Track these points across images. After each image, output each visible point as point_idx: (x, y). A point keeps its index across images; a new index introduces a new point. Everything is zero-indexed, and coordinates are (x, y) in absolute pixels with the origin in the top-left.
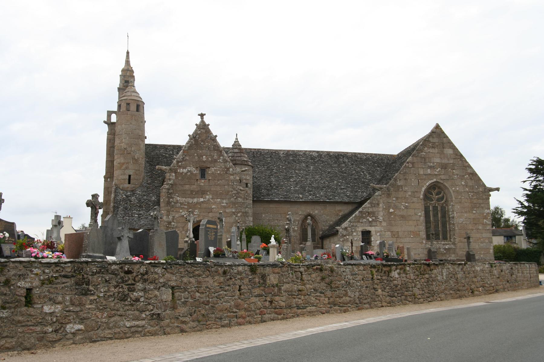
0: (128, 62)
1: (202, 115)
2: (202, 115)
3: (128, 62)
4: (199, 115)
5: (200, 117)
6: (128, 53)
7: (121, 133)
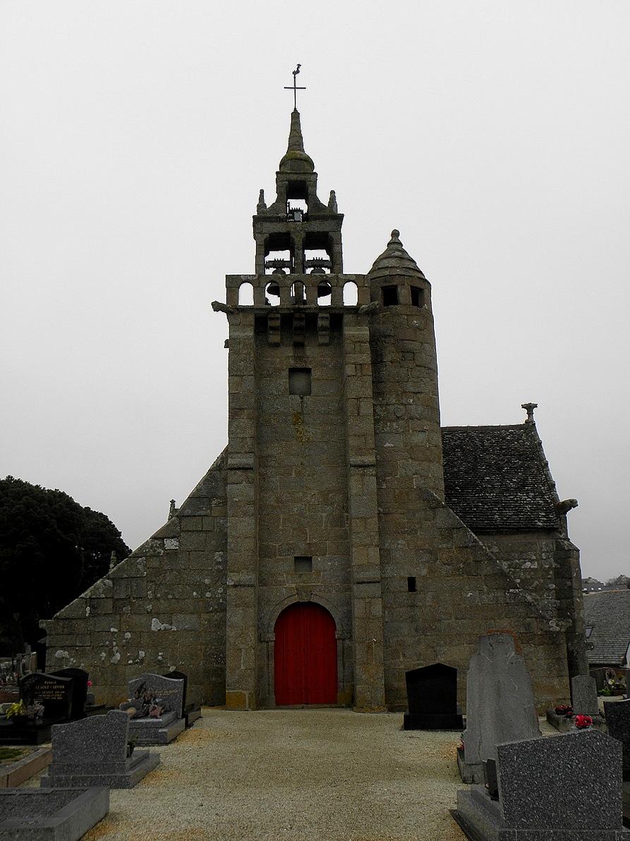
1: (530, 408)
2: (530, 408)
4: (523, 407)
6: (295, 116)
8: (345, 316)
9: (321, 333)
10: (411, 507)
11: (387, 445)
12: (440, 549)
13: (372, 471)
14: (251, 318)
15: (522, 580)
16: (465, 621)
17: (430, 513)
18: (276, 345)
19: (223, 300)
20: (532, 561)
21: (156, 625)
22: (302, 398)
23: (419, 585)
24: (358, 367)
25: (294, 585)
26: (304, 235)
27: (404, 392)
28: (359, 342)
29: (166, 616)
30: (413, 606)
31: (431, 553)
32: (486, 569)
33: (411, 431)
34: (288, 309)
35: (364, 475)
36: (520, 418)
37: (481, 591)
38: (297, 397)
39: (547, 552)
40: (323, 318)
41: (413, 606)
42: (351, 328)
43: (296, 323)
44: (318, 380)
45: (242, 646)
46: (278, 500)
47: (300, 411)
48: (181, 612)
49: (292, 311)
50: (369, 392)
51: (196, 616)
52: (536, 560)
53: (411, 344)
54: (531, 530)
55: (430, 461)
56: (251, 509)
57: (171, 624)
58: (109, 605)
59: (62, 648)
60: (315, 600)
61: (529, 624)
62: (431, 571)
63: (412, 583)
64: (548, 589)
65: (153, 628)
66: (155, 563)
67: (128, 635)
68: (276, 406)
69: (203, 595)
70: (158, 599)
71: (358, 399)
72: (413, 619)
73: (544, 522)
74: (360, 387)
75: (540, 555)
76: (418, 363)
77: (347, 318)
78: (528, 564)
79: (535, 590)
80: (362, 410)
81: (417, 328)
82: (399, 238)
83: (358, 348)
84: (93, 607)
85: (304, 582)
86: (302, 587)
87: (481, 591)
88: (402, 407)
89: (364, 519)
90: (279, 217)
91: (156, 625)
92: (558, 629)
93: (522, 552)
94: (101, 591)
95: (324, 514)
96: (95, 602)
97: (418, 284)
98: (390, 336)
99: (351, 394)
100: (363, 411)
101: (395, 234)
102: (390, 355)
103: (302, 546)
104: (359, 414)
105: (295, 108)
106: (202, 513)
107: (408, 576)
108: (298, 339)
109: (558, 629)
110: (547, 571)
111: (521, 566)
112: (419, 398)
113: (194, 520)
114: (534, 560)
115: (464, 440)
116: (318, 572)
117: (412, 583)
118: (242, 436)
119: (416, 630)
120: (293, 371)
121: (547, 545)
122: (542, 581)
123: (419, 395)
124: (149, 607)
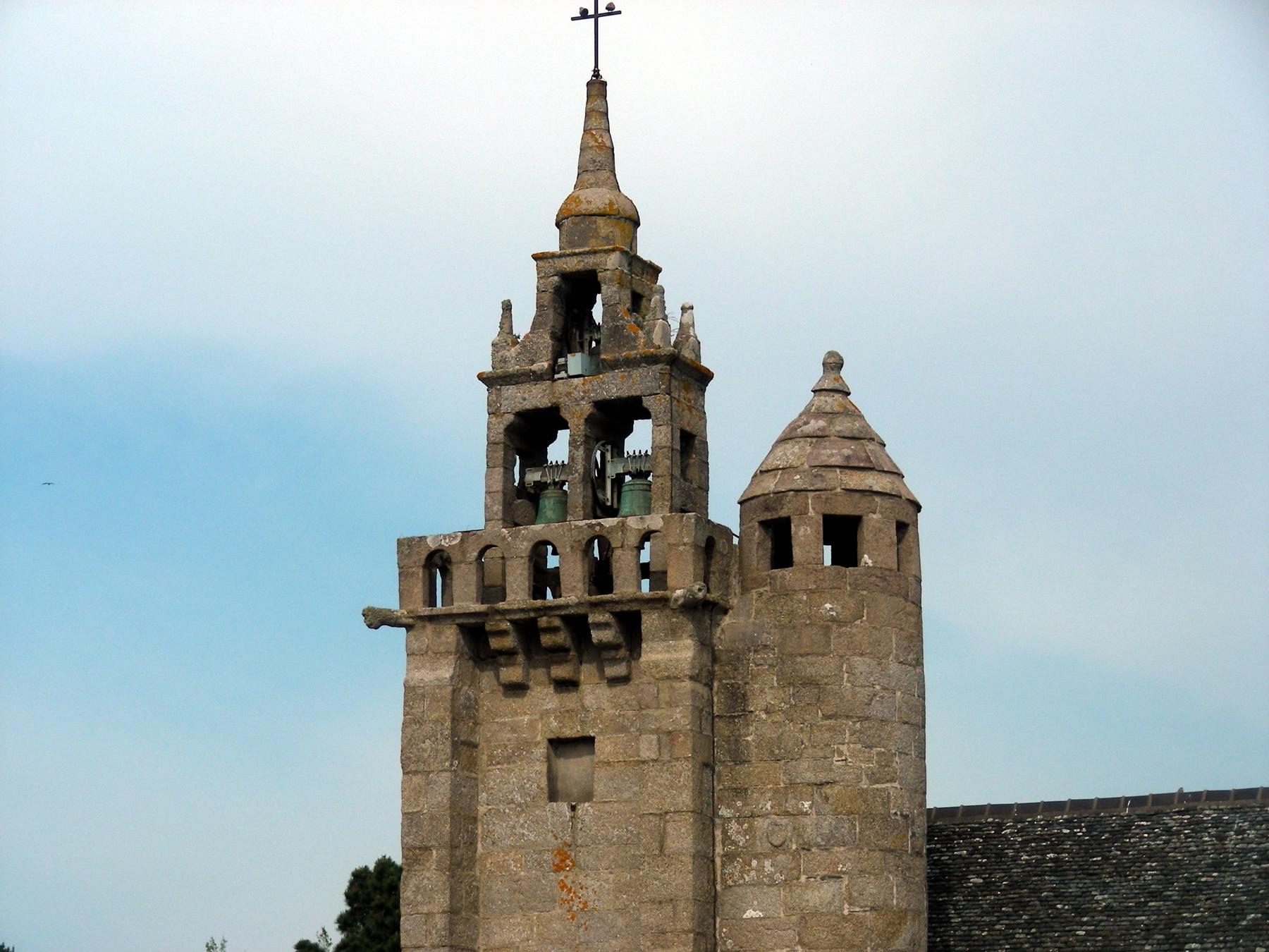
0: (598, 156)
3: (598, 156)
6: (597, 87)
7: (877, 709)
8: (644, 618)
9: (606, 655)
11: (750, 913)
14: (450, 635)
18: (517, 689)
22: (573, 808)
24: (665, 739)
26: (587, 408)
27: (792, 784)
28: (668, 678)
33: (803, 878)
34: (522, 610)
38: (564, 807)
42: (655, 645)
43: (546, 640)
44: (608, 763)
47: (568, 839)
49: (532, 615)
50: (685, 799)
53: (812, 664)
68: (519, 830)
71: (662, 815)
76: (829, 709)
77: (650, 621)
80: (669, 842)
81: (833, 620)
82: (843, 373)
83: (664, 696)
88: (784, 821)
90: (534, 372)
97: (844, 508)
98: (766, 646)
100: (672, 845)
101: (834, 364)
102: (765, 694)
105: (596, 73)
108: (560, 671)
112: (827, 798)
115: (1178, 833)
118: (425, 909)
120: (560, 745)
123: (827, 790)
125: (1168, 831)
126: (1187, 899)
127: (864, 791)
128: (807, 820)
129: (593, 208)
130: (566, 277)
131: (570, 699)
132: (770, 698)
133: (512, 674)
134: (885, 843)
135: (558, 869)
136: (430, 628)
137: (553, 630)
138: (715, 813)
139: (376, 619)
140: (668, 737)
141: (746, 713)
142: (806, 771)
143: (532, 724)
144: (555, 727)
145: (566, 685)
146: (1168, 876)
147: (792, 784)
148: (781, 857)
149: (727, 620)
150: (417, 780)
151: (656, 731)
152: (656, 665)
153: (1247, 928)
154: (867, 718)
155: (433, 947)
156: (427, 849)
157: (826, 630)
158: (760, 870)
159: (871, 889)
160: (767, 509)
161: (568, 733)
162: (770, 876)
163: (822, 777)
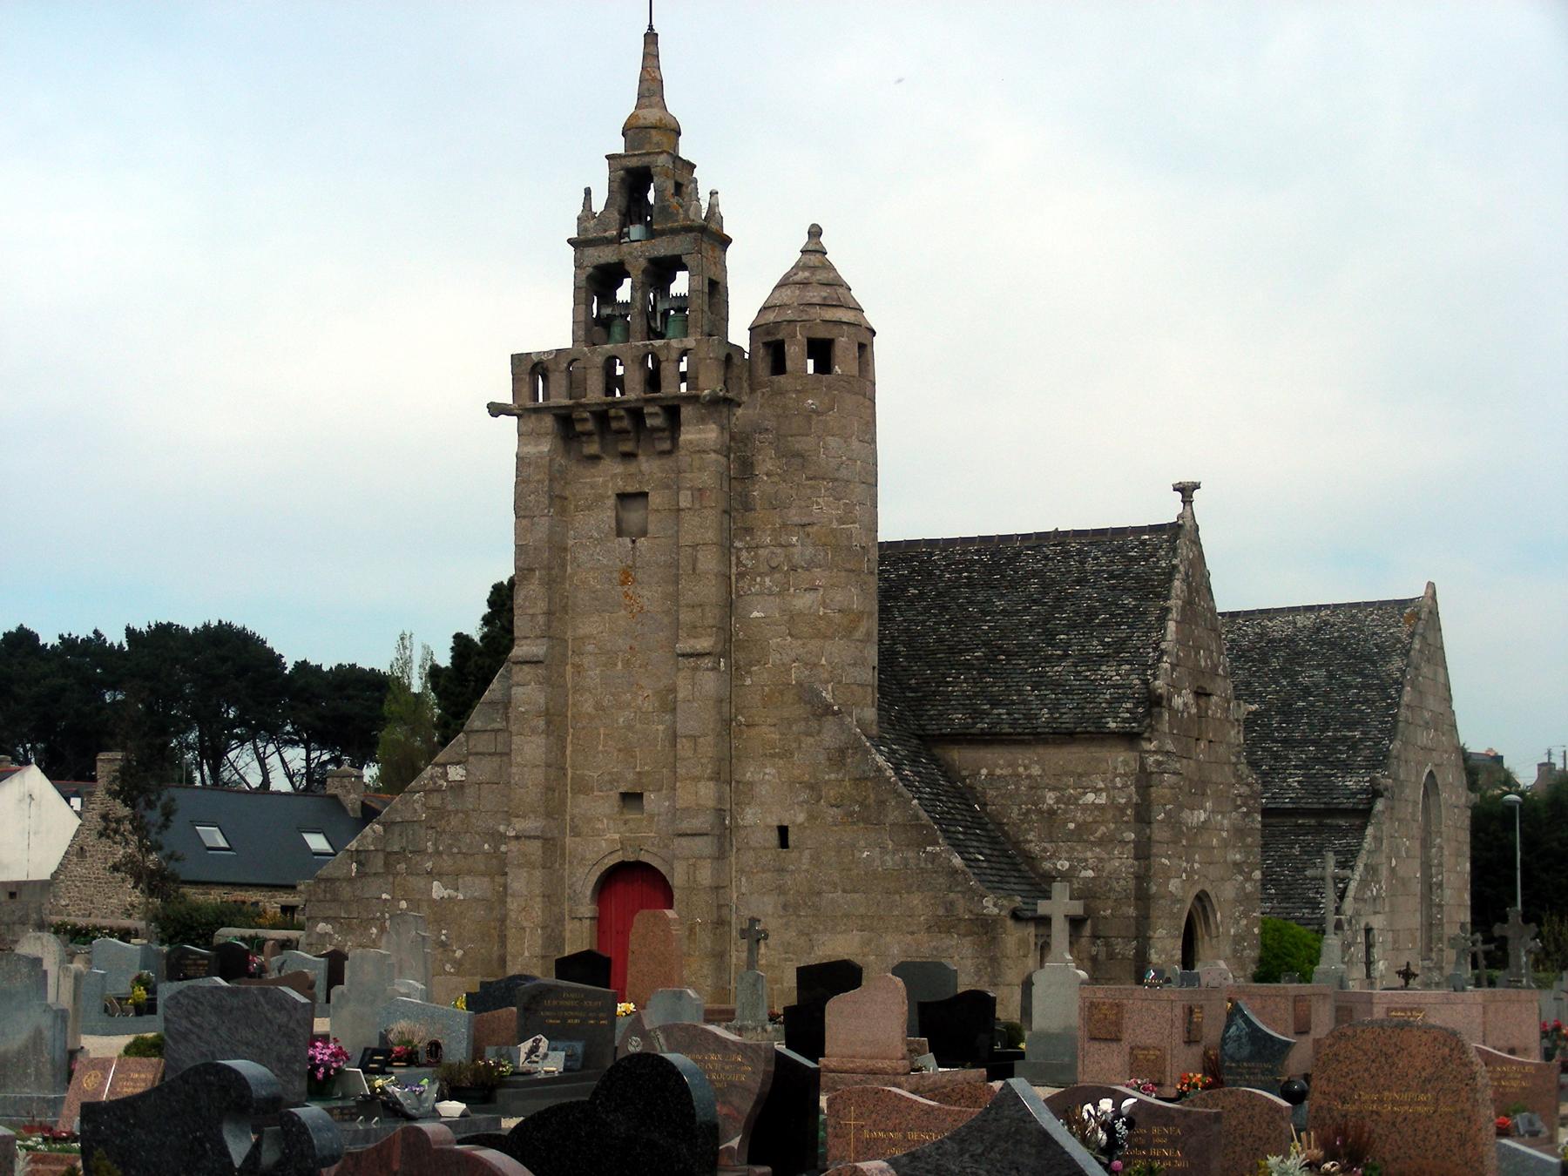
0: (651, 86)
1: (1186, 491)
3: (651, 86)
5: (1179, 495)
6: (651, 37)
9: (656, 435)
10: (786, 715)
11: (755, 614)
12: (826, 782)
13: (707, 662)
14: (548, 422)
15: (1078, 826)
16: (856, 896)
17: (814, 724)
18: (595, 459)
19: (507, 398)
20: (1097, 791)
21: (438, 890)
23: (792, 838)
24: (697, 494)
25: (617, 836)
26: (643, 263)
29: (451, 878)
30: (781, 870)
31: (812, 787)
32: (894, 815)
35: (696, 669)
36: (1167, 510)
37: (884, 849)
38: (628, 540)
39: (1125, 775)
40: (651, 414)
41: (781, 870)
43: (614, 425)
45: (525, 924)
46: (598, 706)
48: (470, 872)
50: (711, 535)
51: (487, 879)
52: (1106, 789)
54: (1100, 736)
55: (825, 637)
56: (542, 723)
57: (457, 890)
58: (378, 863)
59: (326, 920)
60: (645, 858)
61: (952, 903)
62: (811, 817)
63: (783, 831)
64: (1123, 842)
65: (434, 896)
66: (436, 801)
67: (403, 904)
69: (496, 849)
70: (438, 853)
71: (695, 546)
72: (781, 890)
73: (1124, 720)
74: (702, 527)
75: (1112, 781)
77: (686, 412)
78: (1090, 797)
79: (1100, 842)
81: (813, 411)
82: (822, 239)
83: (696, 463)
84: (359, 863)
85: (631, 831)
86: (629, 839)
87: (884, 849)
88: (779, 550)
89: (694, 738)
91: (438, 890)
92: (996, 911)
93: (1080, 776)
94: (369, 840)
95: (661, 727)
96: (362, 857)
97: (821, 333)
99: (686, 540)
100: (701, 567)
101: (815, 232)
102: (766, 463)
103: (631, 776)
104: (694, 569)
106: (496, 726)
107: (776, 823)
108: (627, 447)
109: (996, 911)
110: (1122, 810)
111: (1077, 799)
113: (485, 736)
114: (1101, 790)
116: (651, 817)
117: (783, 831)
119: (785, 907)
120: (623, 497)
121: (1126, 763)
122: (1112, 826)
123: (808, 529)
124: (429, 865)
125: (1046, 558)
126: (1058, 604)
127: (833, 530)
128: (794, 550)
129: (647, 123)
130: (630, 171)
131: (632, 468)
132: (769, 466)
133: (593, 448)
134: (848, 566)
135: (623, 583)
136: (533, 417)
137: (620, 418)
138: (731, 545)
139: (496, 410)
140: (699, 492)
141: (753, 476)
142: (794, 516)
143: (605, 482)
144: (621, 485)
145: (629, 456)
146: (1045, 587)
147: (784, 525)
148: (777, 576)
149: (740, 411)
150: (524, 522)
151: (691, 488)
152: (691, 442)
153: (1099, 625)
154: (836, 480)
155: (537, 637)
156: (533, 570)
157: (809, 419)
158: (762, 584)
159: (839, 598)
160: (768, 333)
161: (630, 489)
162: (770, 589)
163: (805, 520)
